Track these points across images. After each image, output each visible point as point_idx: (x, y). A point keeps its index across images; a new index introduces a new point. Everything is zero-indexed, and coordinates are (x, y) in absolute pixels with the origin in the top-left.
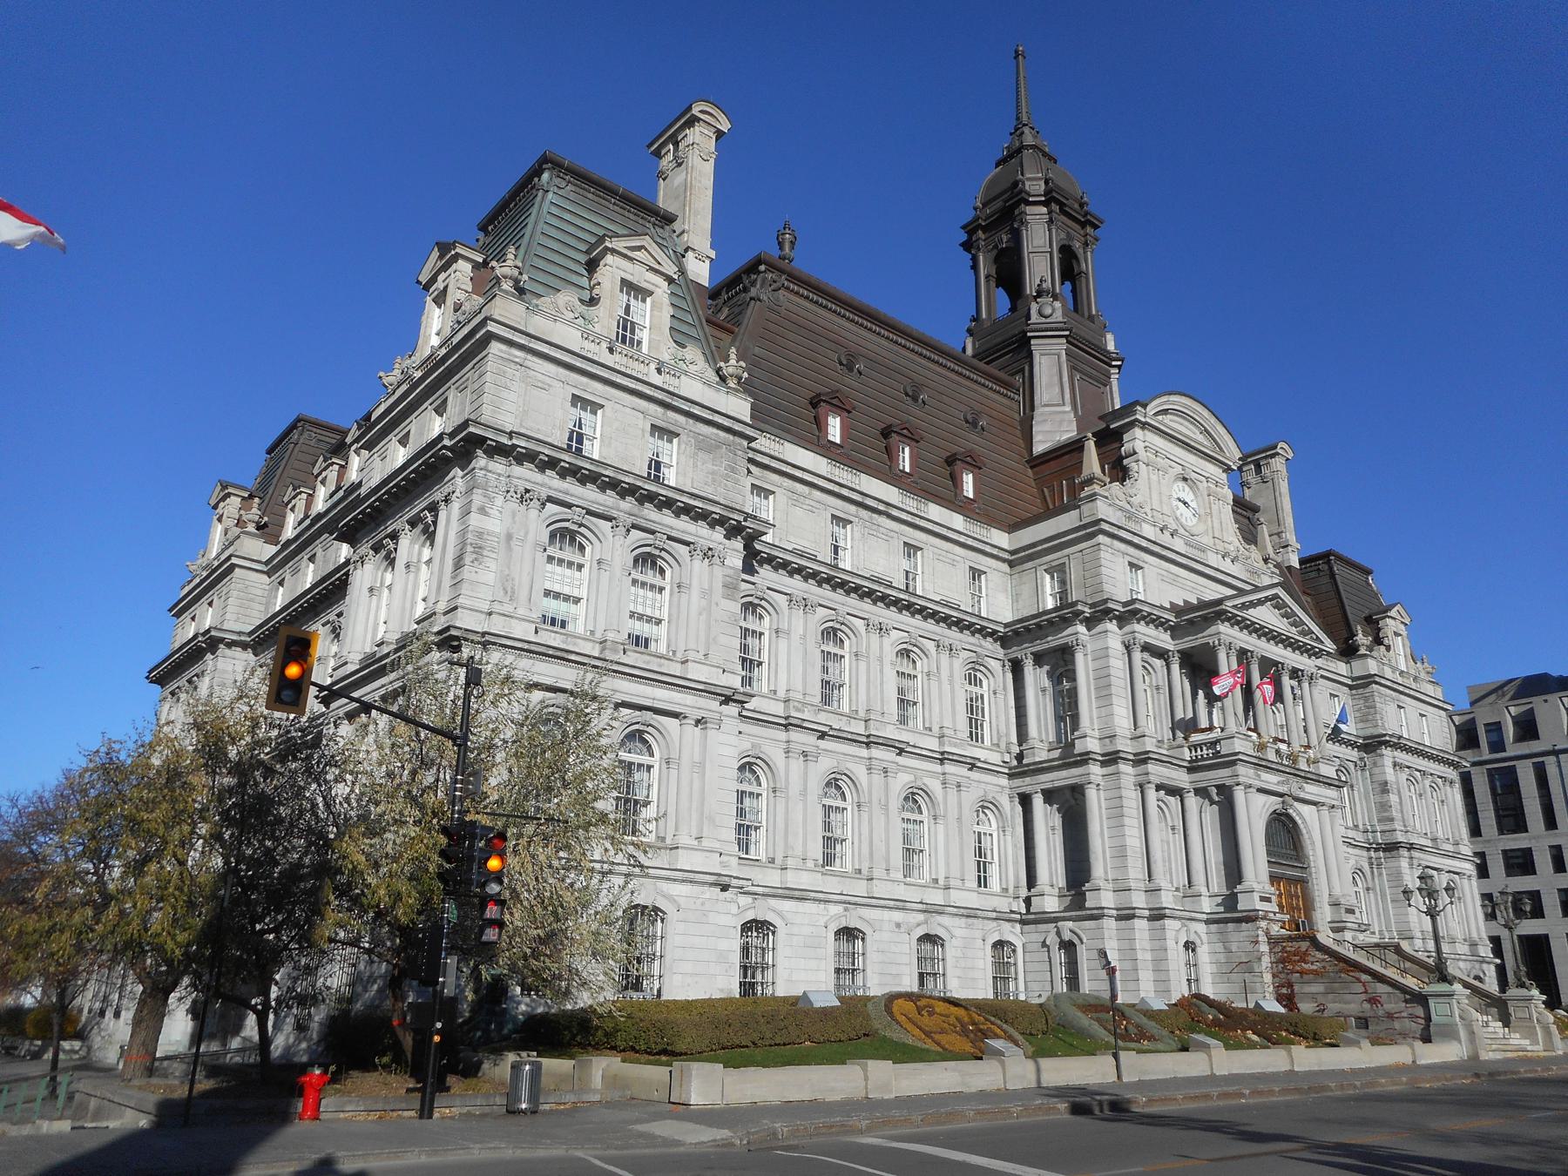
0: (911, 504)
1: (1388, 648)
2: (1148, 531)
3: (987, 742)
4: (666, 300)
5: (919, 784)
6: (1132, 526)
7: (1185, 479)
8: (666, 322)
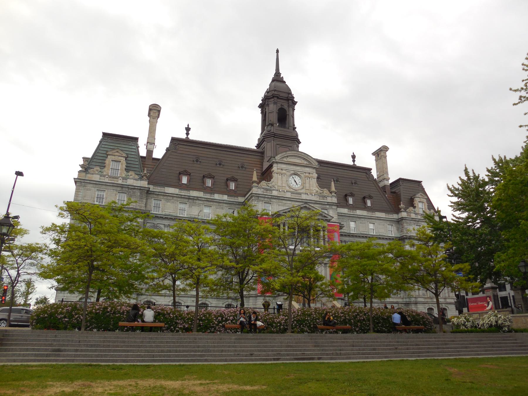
0: (208, 196)
1: (415, 207)
4: (124, 162)
8: (124, 167)
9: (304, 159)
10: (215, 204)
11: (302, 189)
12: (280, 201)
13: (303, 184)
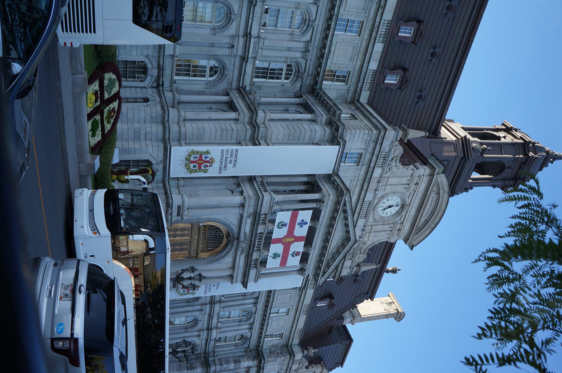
0: (382, 30)
1: (307, 367)
2: (378, 172)
3: (255, 80)
5: (233, 17)
6: (381, 160)
7: (403, 206)
9: (427, 222)
10: (364, 43)
11: (375, 220)
12: (360, 182)
13: (383, 221)
